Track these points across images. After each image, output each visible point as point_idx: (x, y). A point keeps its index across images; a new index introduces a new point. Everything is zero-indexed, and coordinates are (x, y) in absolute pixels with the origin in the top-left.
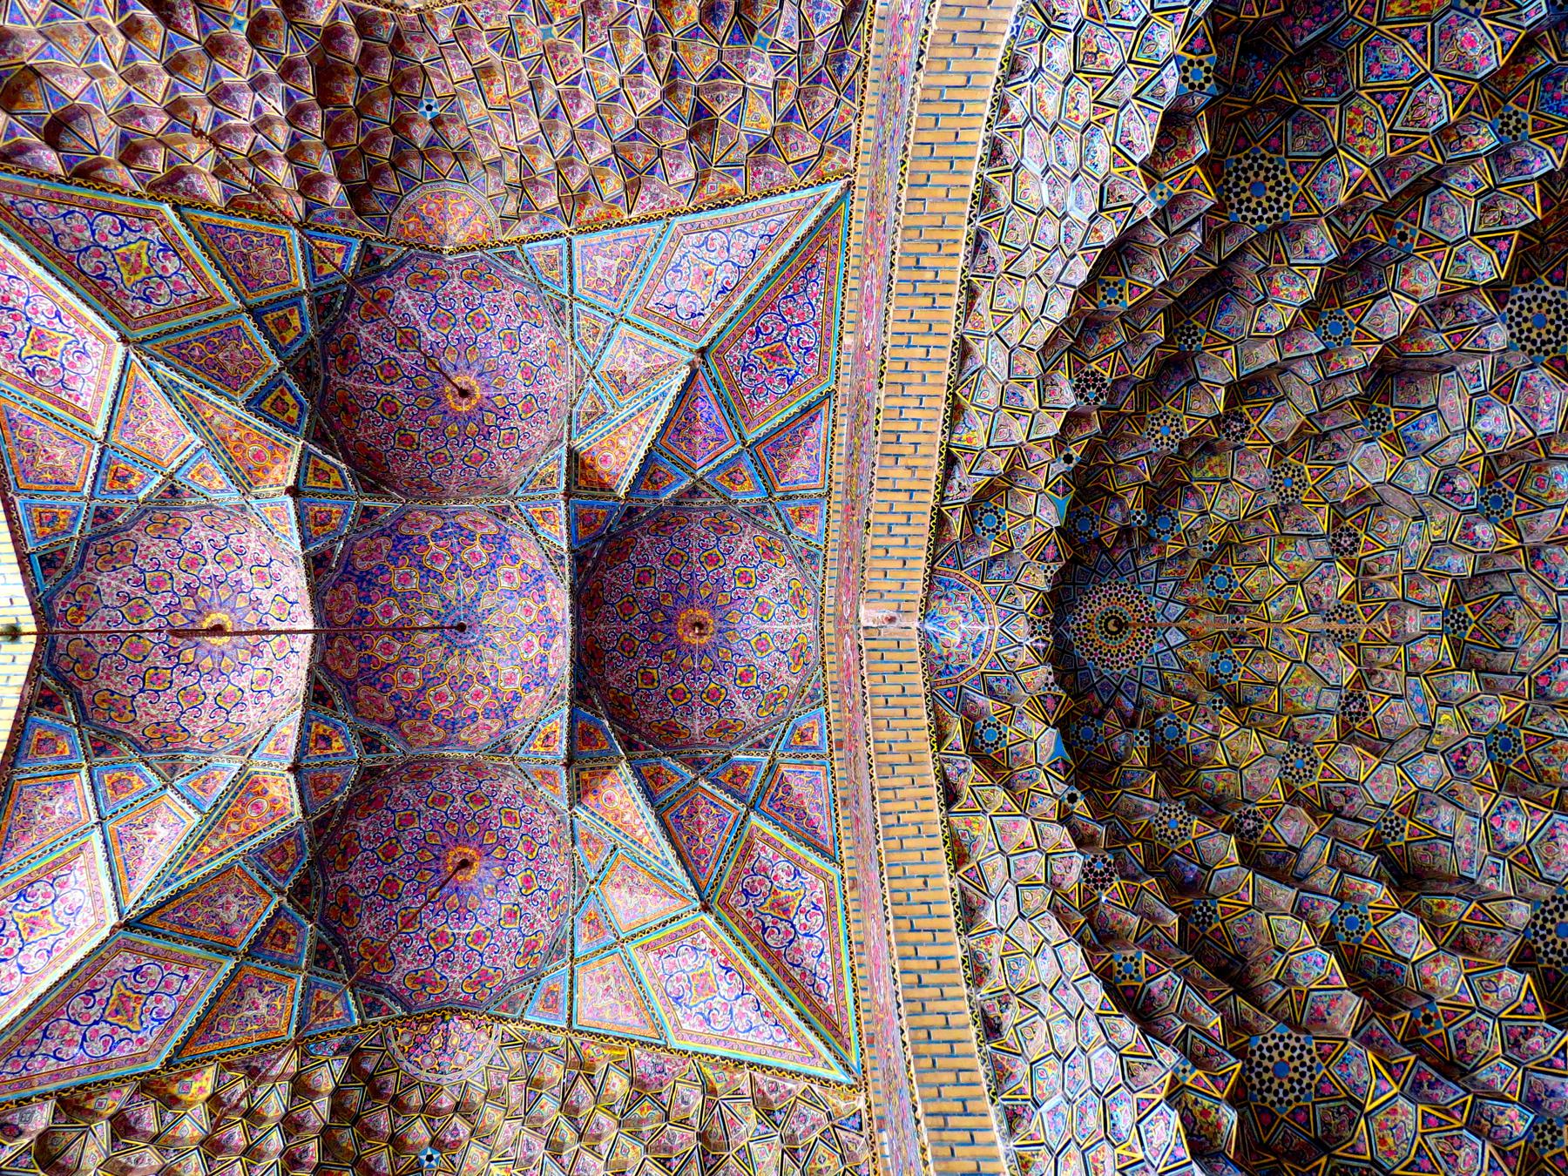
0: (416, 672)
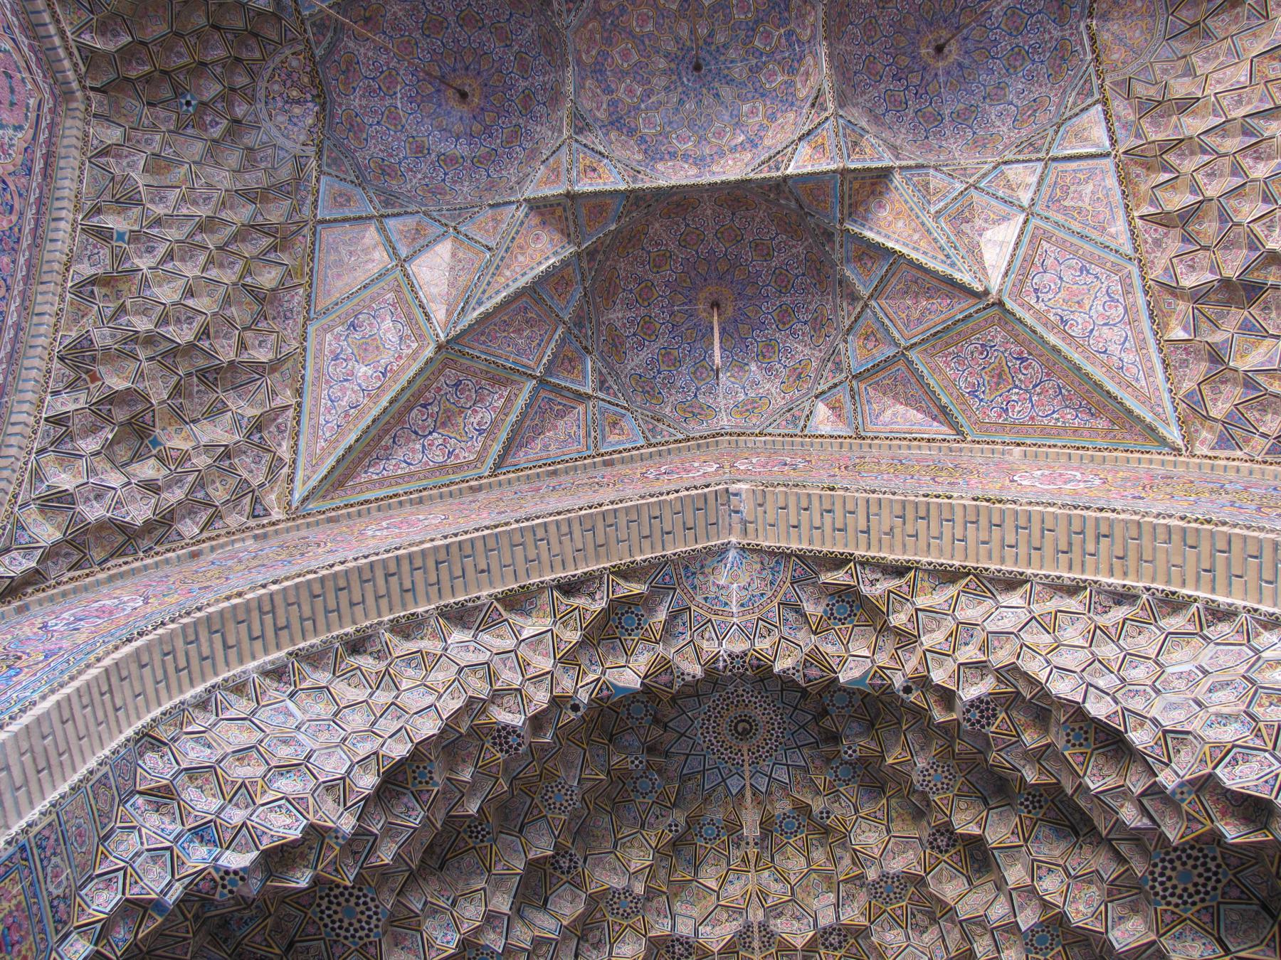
0: (649, 27)
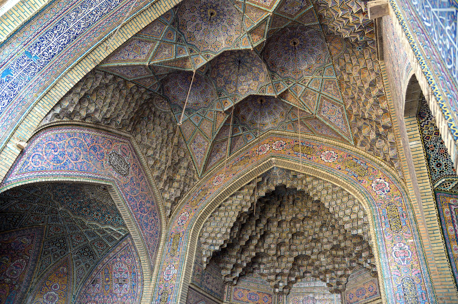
0: (225, 59)
